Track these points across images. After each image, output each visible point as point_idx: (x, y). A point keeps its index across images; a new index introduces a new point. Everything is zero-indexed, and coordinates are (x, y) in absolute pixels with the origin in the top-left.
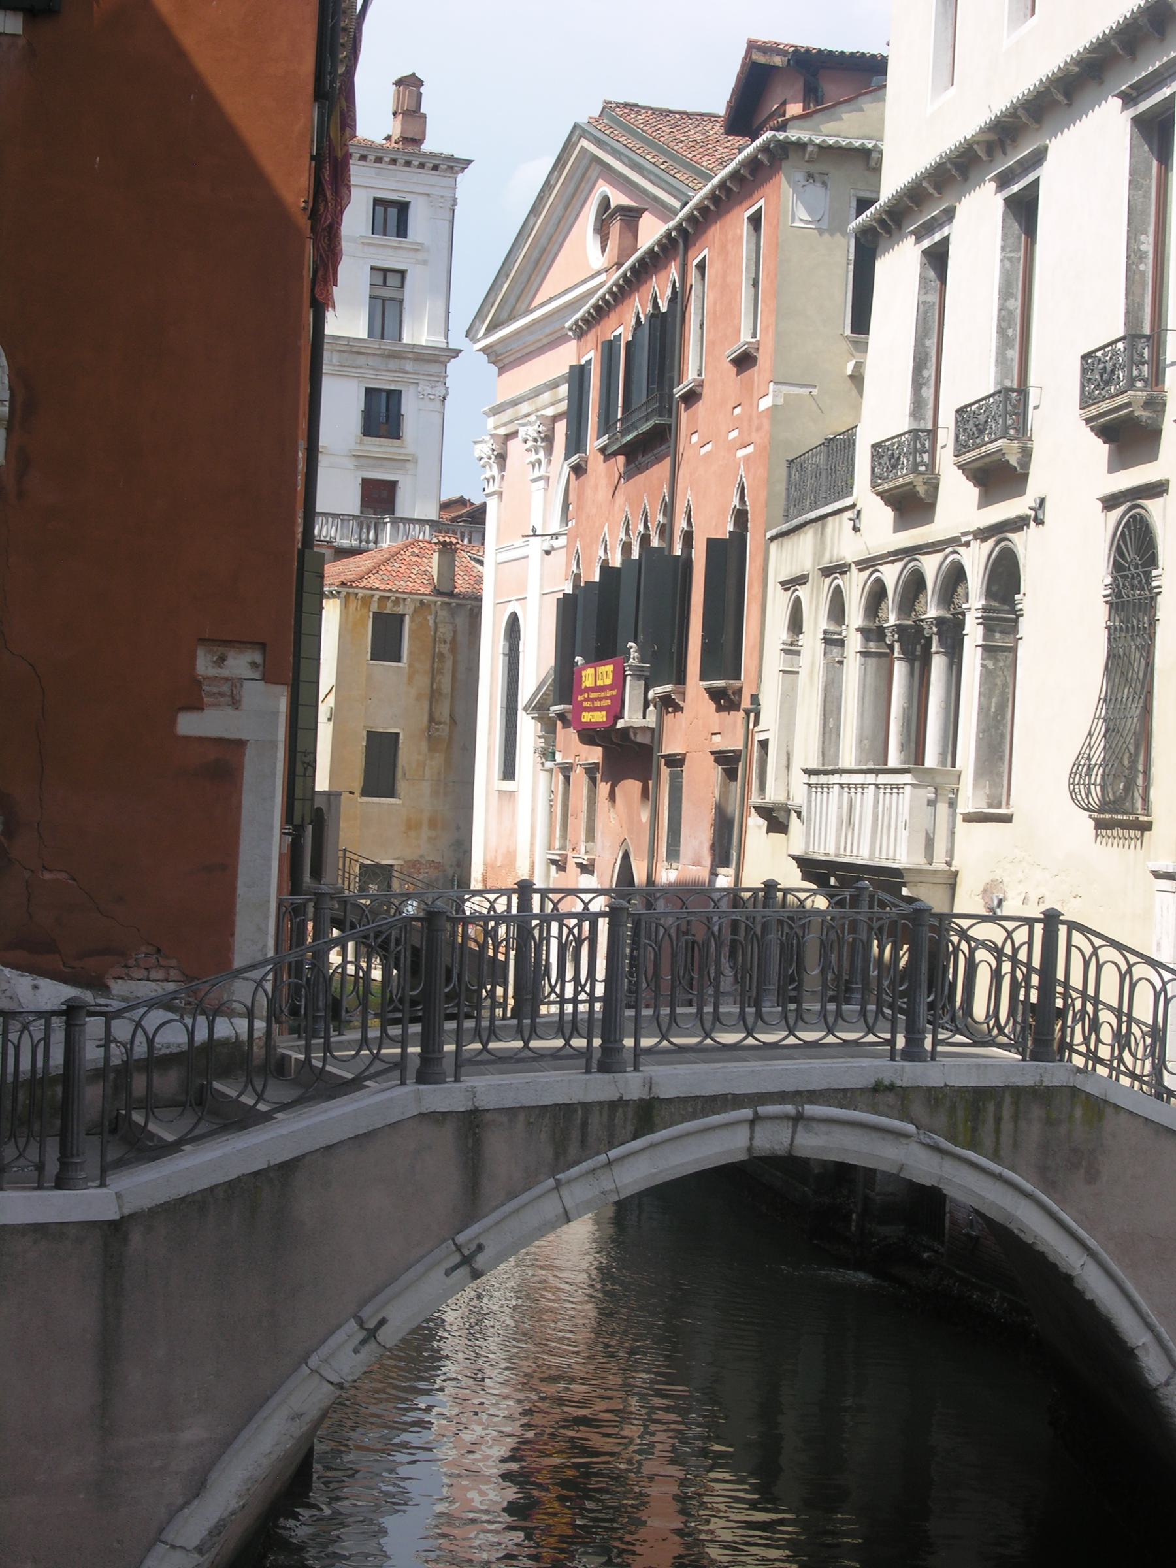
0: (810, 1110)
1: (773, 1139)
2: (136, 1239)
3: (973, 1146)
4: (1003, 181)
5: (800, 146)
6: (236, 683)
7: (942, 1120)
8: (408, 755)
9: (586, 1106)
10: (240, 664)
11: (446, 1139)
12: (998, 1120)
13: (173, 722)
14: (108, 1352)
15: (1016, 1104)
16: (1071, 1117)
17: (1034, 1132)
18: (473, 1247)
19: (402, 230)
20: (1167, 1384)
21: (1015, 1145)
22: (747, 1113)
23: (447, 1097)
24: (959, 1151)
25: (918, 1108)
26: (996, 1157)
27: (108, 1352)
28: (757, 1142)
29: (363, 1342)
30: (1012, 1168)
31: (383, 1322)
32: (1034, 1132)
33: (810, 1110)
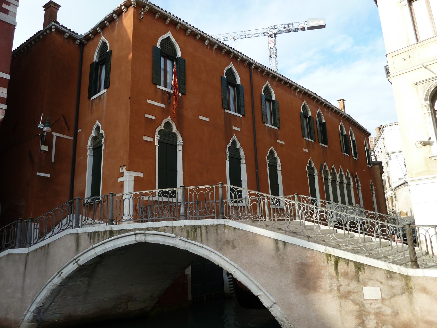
0: (147, 232)
1: (141, 238)
3: (194, 239)
7: (185, 233)
9: (98, 232)
10: (124, 169)
14: (24, 275)
15: (206, 229)
16: (224, 232)
17: (212, 236)
18: (78, 259)
20: (271, 307)
21: (207, 240)
22: (133, 233)
24: (188, 241)
25: (177, 231)
26: (202, 242)
27: (24, 275)
30: (208, 245)
31: (62, 273)
33: (147, 232)
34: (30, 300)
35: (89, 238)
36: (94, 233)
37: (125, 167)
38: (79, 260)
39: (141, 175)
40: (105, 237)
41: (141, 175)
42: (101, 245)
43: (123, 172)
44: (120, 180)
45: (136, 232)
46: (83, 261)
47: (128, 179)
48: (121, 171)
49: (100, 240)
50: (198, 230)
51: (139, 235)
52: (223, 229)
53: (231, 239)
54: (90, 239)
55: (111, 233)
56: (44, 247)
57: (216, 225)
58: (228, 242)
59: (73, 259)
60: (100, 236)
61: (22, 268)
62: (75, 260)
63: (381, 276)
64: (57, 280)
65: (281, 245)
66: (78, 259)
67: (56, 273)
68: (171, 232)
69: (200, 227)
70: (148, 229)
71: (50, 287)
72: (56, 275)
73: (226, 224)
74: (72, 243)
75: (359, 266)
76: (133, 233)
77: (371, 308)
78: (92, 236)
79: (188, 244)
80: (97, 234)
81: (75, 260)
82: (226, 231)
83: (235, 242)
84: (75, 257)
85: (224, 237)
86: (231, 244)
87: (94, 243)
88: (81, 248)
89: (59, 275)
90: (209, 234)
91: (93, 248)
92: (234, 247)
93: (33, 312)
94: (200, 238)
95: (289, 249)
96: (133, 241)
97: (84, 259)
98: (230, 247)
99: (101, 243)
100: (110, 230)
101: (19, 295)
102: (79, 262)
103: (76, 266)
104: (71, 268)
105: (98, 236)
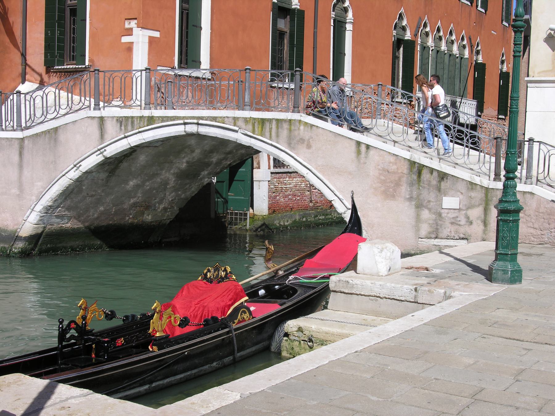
0: (201, 122)
2: (26, 142)
6: (131, 29)
7: (250, 127)
9: (132, 117)
10: (133, 24)
11: (95, 123)
12: (271, 129)
13: (121, 40)
14: (21, 166)
16: (299, 129)
17: (284, 133)
20: (344, 213)
21: (278, 136)
23: (97, 114)
25: (240, 123)
26: (270, 138)
27: (21, 166)
28: (186, 130)
29: (76, 170)
30: (277, 143)
31: (80, 166)
32: (284, 133)
34: (34, 198)
35: (119, 124)
36: (127, 118)
37: (136, 21)
38: (105, 150)
39: (157, 34)
40: (142, 123)
41: (157, 34)
42: (136, 134)
43: (131, 29)
44: (125, 39)
45: (186, 121)
46: (110, 152)
47: (140, 39)
48: (127, 26)
49: (135, 128)
50: (267, 125)
51: (189, 125)
52: (297, 124)
53: (307, 138)
54: (121, 126)
55: (151, 120)
56: (48, 132)
57: (290, 120)
58: (302, 141)
59: (96, 149)
60: (136, 123)
61: (16, 158)
62: (99, 150)
63: (461, 187)
64: (74, 174)
65: (363, 148)
66: (103, 150)
67: (72, 166)
68: (232, 124)
69: (270, 120)
70: (202, 118)
72: (72, 168)
73: (302, 119)
74: (94, 128)
75: (443, 176)
76: (182, 122)
77: (448, 216)
78: (122, 121)
79: (253, 140)
80: (130, 120)
81: (99, 150)
82: (302, 128)
83: (310, 141)
84: (99, 147)
85: (299, 134)
86: (306, 143)
87: (126, 130)
88: (106, 136)
89: (75, 168)
90: (280, 130)
91: (126, 137)
92: (309, 147)
93: (40, 212)
94: (269, 133)
95: (372, 152)
96: (182, 131)
97: (112, 151)
98: (305, 145)
99: (137, 131)
100: (149, 117)
101: (15, 191)
102: (105, 154)
103: (100, 158)
104: (95, 160)
105: (133, 123)
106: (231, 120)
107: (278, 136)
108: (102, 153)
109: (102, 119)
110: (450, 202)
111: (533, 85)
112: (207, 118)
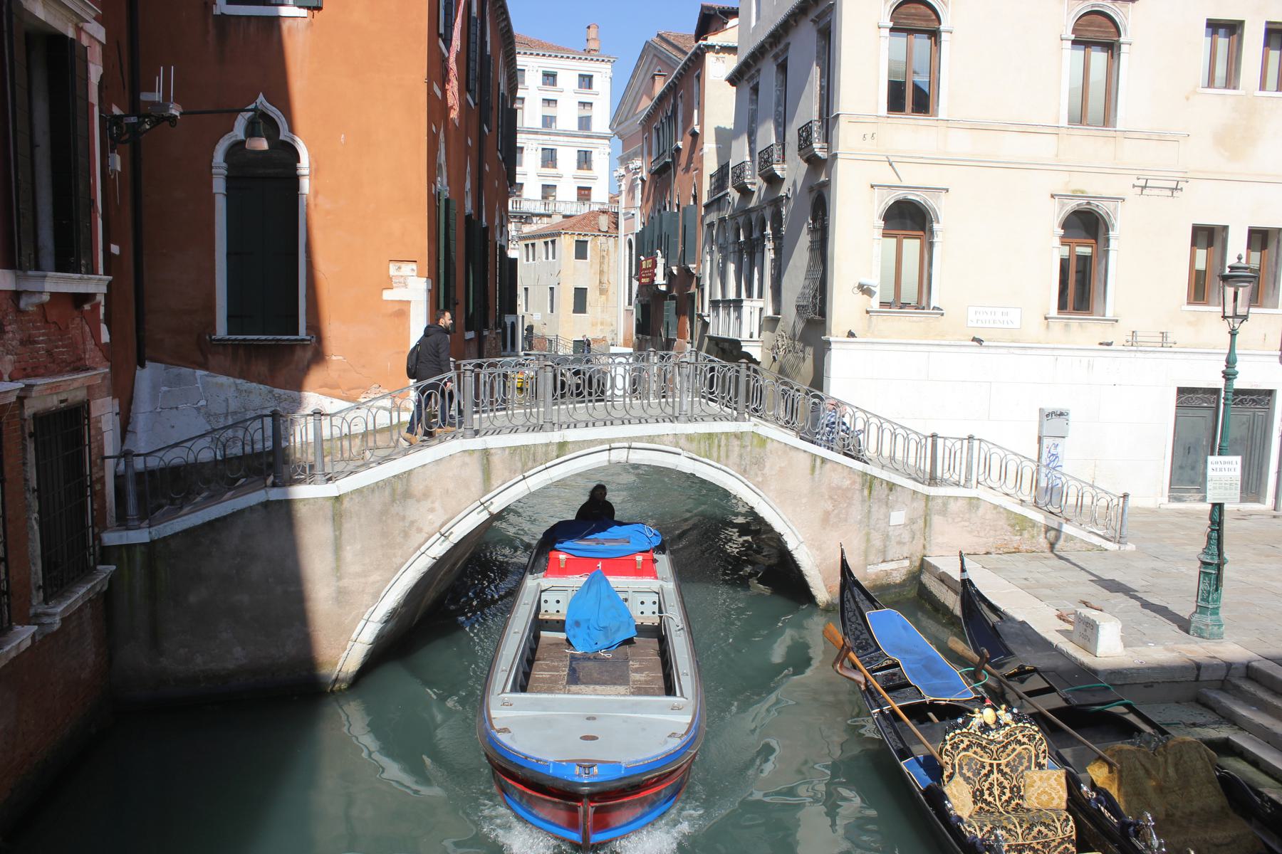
0: (634, 445)
2: (346, 503)
4: (776, 57)
5: (711, 48)
6: (405, 277)
8: (590, 297)
12: (719, 446)
19: (590, 87)
21: (727, 456)
26: (718, 461)
37: (414, 266)
64: (440, 549)
65: (818, 462)
71: (422, 564)
74: (473, 471)
75: (891, 486)
84: (483, 500)
95: (828, 466)
99: (543, 467)
106: (671, 438)
107: (727, 456)
108: (486, 508)
109: (486, 453)
110: (898, 517)
111: (838, 346)
112: (640, 439)
